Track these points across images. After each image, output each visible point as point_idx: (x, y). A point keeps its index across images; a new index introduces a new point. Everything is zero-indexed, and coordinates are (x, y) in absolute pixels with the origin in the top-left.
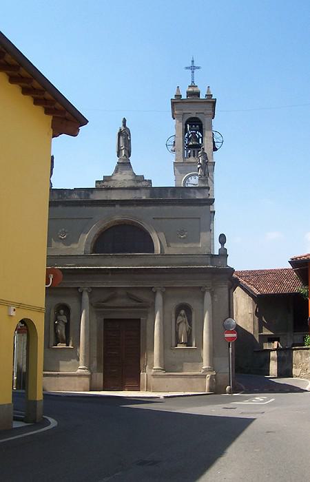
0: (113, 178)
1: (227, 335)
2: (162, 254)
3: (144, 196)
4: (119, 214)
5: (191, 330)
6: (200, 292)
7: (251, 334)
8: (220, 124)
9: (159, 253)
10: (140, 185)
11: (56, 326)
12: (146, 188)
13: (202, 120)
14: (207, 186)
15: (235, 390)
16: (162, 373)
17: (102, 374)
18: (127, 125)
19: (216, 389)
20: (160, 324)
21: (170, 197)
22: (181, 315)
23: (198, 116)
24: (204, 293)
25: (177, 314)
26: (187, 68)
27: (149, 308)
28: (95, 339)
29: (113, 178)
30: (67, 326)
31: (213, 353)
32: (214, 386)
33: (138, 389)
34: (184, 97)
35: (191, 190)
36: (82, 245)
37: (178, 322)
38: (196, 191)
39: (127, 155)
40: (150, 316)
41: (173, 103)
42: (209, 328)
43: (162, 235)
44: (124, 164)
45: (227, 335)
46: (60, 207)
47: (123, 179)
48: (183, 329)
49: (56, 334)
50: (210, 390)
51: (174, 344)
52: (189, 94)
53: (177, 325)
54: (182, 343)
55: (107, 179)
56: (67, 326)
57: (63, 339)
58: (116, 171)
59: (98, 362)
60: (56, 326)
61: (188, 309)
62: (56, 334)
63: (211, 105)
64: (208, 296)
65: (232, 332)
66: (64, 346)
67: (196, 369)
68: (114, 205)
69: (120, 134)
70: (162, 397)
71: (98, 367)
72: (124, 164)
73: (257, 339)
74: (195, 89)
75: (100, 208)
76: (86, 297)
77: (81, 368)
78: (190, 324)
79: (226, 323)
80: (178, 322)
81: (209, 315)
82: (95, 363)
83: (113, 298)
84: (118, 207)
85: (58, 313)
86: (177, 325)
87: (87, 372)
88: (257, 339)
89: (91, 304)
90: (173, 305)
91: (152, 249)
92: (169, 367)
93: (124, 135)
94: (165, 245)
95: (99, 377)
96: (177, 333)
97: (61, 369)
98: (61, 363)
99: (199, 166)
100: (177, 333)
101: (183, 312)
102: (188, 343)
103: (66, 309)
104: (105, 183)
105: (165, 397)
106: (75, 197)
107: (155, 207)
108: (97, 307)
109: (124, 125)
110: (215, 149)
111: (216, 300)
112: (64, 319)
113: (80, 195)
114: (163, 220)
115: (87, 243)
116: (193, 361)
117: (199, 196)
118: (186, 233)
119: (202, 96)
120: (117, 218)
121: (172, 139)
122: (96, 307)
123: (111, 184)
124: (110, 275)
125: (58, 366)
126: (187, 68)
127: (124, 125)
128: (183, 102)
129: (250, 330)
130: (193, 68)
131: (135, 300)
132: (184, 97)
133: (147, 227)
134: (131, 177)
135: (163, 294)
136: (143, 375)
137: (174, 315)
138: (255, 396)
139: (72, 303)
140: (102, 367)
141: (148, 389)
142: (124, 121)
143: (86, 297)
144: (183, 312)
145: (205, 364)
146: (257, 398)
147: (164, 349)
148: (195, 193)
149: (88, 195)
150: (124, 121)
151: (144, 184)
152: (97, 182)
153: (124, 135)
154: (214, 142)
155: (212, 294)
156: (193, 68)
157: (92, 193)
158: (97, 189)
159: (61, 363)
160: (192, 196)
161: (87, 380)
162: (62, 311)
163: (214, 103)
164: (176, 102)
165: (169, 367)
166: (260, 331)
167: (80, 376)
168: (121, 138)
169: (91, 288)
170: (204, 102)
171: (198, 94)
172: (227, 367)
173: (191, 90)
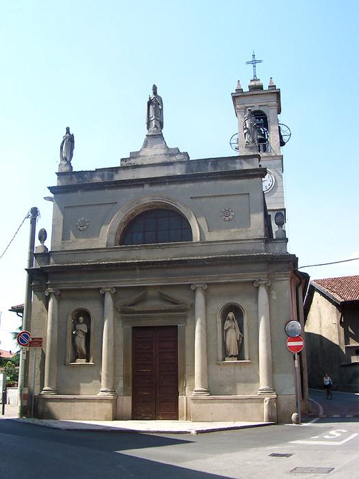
0: (141, 154)
1: (290, 344)
2: (203, 241)
3: (178, 171)
4: (147, 197)
5: (243, 338)
6: (253, 287)
7: (336, 345)
8: (289, 117)
9: (199, 240)
10: (174, 159)
11: (74, 337)
12: (181, 162)
15: (306, 416)
16: (205, 396)
17: (130, 398)
18: (158, 94)
19: (278, 418)
20: (201, 331)
21: (210, 169)
22: (229, 319)
24: (257, 288)
25: (224, 318)
26: (248, 63)
27: (187, 311)
28: (121, 352)
29: (141, 154)
30: (88, 336)
31: (273, 368)
32: (275, 414)
33: (174, 416)
34: (246, 89)
35: (238, 161)
36: (105, 236)
37: (225, 328)
38: (243, 161)
39: (158, 126)
40: (189, 321)
41: (234, 98)
42: (267, 333)
43: (202, 221)
44: (156, 136)
45: (290, 344)
46: (79, 193)
47: (155, 153)
48: (232, 337)
49: (75, 347)
50: (270, 418)
51: (220, 357)
53: (224, 332)
54: (232, 356)
55: (134, 155)
56: (88, 336)
57: (83, 354)
58: (145, 145)
59: (125, 382)
60: (74, 337)
61: (237, 311)
62: (75, 347)
63: (274, 97)
64: (263, 292)
65: (297, 339)
66: (83, 362)
67: (252, 390)
68: (142, 185)
69: (150, 103)
70: (193, 432)
71: (125, 389)
72: (156, 136)
73: (344, 351)
74: (257, 83)
75: (126, 191)
76: (109, 300)
77: (101, 389)
78: (241, 331)
79: (289, 327)
80: (225, 328)
81: (266, 322)
82: (121, 384)
83: (142, 300)
84: (147, 187)
85: (76, 322)
86: (224, 332)
87: (110, 396)
88: (344, 351)
89: (115, 308)
90: (218, 305)
91: (190, 237)
92: (213, 389)
93: (155, 104)
94: (205, 229)
95: (126, 403)
96: (224, 343)
97: (81, 393)
98: (82, 385)
99: (245, 131)
100: (224, 343)
101: (231, 315)
102: (240, 356)
103: (86, 315)
104: (132, 161)
105: (198, 432)
106: (97, 179)
107: (192, 184)
108: (123, 312)
109: (155, 93)
110: (282, 144)
111: (274, 297)
112: (84, 328)
113: (102, 177)
114: (203, 200)
115: (110, 233)
116: (246, 381)
117: (246, 166)
118: (232, 214)
119: (266, 88)
120: (147, 200)
121: (236, 137)
122: (123, 312)
123: (138, 161)
124: (138, 271)
125: (79, 387)
126: (248, 63)
127: (155, 93)
129: (336, 342)
130: (254, 62)
131: (171, 302)
132: (246, 89)
133: (183, 210)
134: (163, 151)
135: (206, 292)
136: (182, 400)
137: (219, 320)
138: (331, 428)
139: (92, 307)
140: (130, 388)
141: (188, 417)
142: (155, 88)
143: (109, 300)
144: (231, 315)
145: (263, 383)
146: (332, 432)
147: (208, 364)
148: (241, 164)
149: (112, 176)
150: (155, 88)
151: (178, 157)
152: (122, 160)
153: (155, 104)
154: (281, 137)
156: (254, 62)
157: (117, 173)
158: (123, 168)
159: (82, 385)
160: (238, 167)
161: (109, 406)
162: (81, 319)
163: (278, 94)
164: (238, 96)
165: (213, 389)
166: (347, 342)
167: (101, 400)
168: (151, 107)
169: (116, 288)
170: (267, 94)
171: (261, 87)
172: (290, 387)
173: (253, 83)
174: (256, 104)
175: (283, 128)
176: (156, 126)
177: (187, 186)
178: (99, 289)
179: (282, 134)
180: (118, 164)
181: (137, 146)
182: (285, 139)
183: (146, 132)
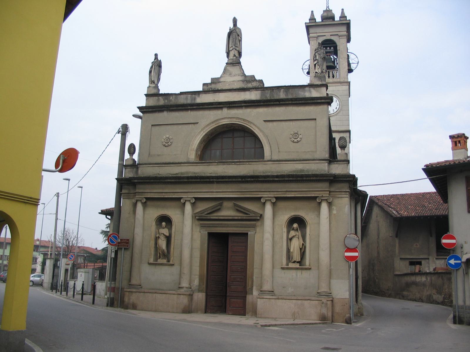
0: (222, 80)
1: (347, 254)
3: (254, 96)
5: (305, 248)
10: (250, 85)
11: (157, 239)
13: (338, 44)
14: (324, 83)
17: (204, 294)
18: (239, 25)
22: (293, 229)
23: (333, 38)
24: (320, 204)
34: (319, 19)
35: (307, 89)
38: (312, 89)
39: (237, 55)
40: (258, 229)
41: (308, 27)
45: (347, 254)
47: (234, 80)
48: (296, 244)
52: (323, 18)
54: (294, 262)
55: (215, 81)
63: (344, 28)
64: (324, 206)
68: (221, 108)
76: (188, 207)
80: (290, 236)
90: (284, 217)
96: (288, 250)
100: (288, 250)
104: (213, 86)
110: (350, 71)
111: (334, 212)
117: (315, 93)
119: (337, 18)
123: (219, 86)
128: (318, 26)
132: (319, 19)
134: (241, 78)
135: (274, 204)
137: (285, 230)
139: (173, 213)
142: (235, 21)
143: (188, 207)
144: (295, 225)
147: (273, 268)
148: (310, 91)
149: (195, 99)
150: (235, 21)
151: (254, 84)
152: (204, 85)
154: (349, 65)
155: (330, 204)
158: (204, 92)
160: (307, 95)
163: (348, 25)
171: (333, 18)
174: (327, 33)
175: (351, 56)
176: (235, 55)
177: (261, 110)
178: (180, 199)
179: (351, 62)
180: (200, 89)
181: (218, 74)
182: (353, 66)
183: (226, 60)
